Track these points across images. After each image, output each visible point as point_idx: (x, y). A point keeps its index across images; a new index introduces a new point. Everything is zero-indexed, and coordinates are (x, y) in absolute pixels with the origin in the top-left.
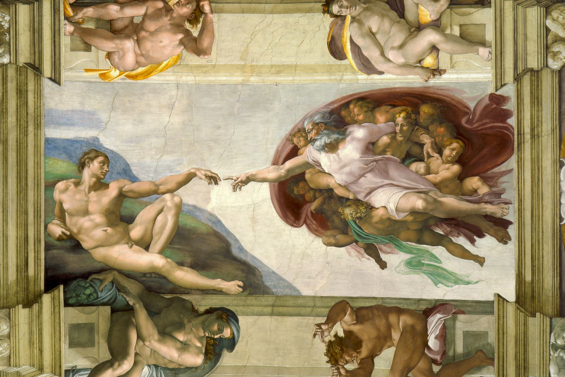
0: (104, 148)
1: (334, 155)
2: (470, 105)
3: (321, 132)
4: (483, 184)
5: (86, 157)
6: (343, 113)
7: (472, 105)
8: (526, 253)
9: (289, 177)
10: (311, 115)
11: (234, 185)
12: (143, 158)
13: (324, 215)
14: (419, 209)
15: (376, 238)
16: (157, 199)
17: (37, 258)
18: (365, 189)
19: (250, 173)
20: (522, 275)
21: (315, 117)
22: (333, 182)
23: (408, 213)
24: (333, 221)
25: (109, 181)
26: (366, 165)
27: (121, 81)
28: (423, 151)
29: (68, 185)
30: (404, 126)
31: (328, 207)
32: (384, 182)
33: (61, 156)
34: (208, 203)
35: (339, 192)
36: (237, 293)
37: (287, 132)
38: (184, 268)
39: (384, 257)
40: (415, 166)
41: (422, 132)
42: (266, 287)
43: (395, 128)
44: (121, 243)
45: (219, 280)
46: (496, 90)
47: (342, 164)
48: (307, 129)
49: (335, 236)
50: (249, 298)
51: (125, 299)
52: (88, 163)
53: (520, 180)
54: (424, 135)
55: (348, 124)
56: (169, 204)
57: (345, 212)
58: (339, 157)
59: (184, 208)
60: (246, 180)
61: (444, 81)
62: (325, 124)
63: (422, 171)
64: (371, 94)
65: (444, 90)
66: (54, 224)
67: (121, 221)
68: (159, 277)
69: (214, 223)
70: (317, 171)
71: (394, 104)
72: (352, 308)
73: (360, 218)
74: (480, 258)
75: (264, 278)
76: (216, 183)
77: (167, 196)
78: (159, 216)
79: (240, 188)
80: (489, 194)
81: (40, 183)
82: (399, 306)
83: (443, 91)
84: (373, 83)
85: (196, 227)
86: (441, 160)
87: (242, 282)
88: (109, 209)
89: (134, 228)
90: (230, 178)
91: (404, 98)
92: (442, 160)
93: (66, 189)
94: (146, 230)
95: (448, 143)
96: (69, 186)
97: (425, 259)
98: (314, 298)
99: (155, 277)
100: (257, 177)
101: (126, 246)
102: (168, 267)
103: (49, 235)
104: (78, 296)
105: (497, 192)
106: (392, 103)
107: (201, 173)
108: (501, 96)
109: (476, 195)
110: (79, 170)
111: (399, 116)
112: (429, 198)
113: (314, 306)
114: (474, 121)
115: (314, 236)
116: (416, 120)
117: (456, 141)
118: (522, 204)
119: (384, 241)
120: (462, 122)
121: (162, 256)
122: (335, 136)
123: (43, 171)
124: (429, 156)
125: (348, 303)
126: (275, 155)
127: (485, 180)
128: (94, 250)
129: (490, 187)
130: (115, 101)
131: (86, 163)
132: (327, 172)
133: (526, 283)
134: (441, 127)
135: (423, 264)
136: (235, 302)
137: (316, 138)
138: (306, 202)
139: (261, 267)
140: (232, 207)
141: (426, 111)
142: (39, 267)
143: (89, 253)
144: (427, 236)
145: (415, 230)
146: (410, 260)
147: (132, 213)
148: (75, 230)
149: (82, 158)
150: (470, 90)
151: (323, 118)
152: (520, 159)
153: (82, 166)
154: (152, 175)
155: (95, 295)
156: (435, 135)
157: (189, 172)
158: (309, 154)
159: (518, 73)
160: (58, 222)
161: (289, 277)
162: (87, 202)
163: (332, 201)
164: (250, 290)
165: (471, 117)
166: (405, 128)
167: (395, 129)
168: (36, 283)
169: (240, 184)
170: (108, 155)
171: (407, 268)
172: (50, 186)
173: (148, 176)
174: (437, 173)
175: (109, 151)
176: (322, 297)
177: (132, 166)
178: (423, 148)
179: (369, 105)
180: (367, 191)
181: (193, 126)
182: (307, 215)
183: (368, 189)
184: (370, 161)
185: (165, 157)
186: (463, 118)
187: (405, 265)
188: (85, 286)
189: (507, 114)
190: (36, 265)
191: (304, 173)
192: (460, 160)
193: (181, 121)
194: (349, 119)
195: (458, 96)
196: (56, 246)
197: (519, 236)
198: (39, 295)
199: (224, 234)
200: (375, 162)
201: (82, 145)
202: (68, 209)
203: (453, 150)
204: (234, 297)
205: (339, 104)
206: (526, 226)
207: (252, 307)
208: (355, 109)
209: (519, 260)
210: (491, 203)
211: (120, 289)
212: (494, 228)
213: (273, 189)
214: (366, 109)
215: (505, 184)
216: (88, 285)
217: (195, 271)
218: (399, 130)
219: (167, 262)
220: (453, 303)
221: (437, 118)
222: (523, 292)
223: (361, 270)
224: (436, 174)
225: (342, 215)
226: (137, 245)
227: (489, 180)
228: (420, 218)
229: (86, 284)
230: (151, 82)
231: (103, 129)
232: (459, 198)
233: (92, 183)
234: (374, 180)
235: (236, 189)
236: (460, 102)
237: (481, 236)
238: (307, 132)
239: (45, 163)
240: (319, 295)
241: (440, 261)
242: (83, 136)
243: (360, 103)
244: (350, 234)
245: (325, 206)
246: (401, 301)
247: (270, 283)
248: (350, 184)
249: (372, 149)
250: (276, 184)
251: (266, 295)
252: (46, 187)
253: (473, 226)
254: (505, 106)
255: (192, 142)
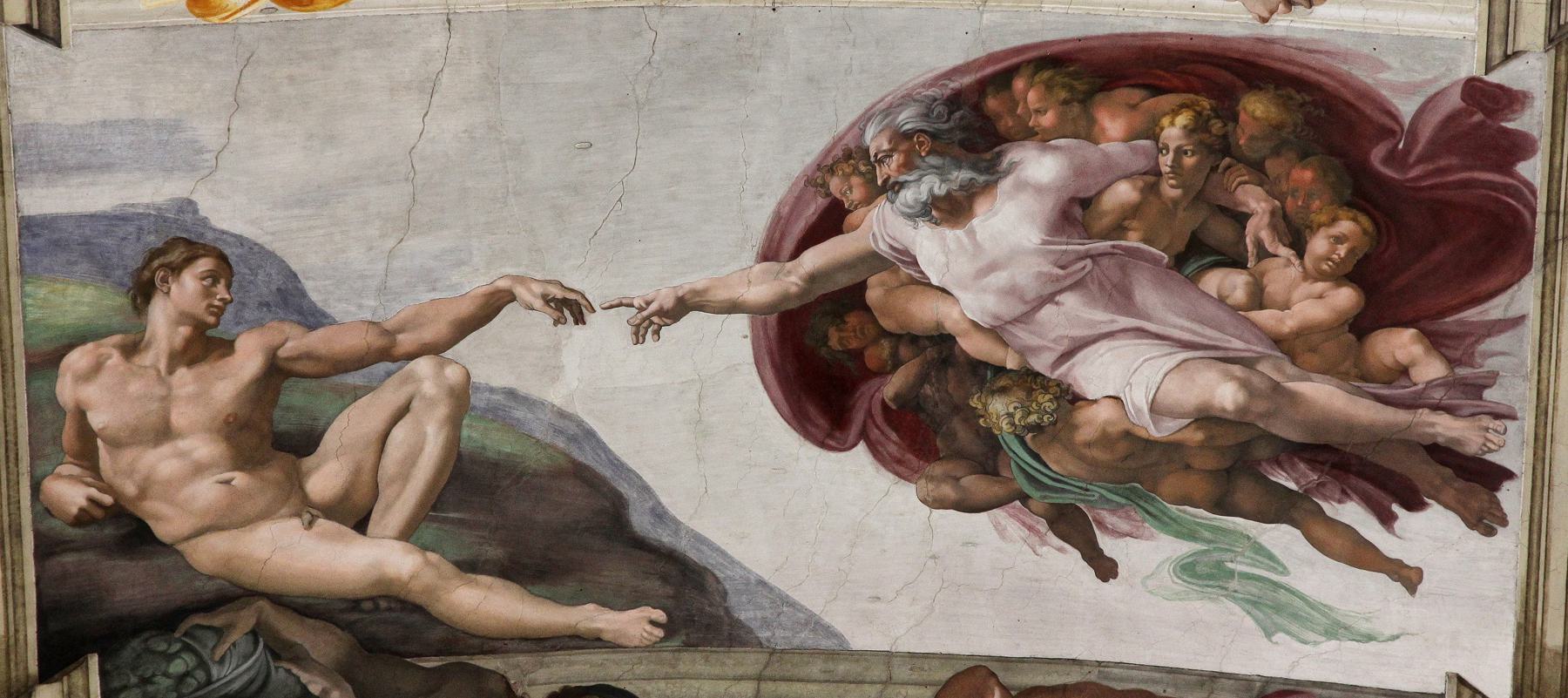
0: (215, 230)
1: (959, 232)
2: (1400, 107)
3: (918, 162)
4: (1427, 351)
5: (156, 263)
6: (992, 103)
7: (1407, 109)
8: (1552, 567)
9: (812, 298)
10: (888, 108)
11: (638, 321)
12: (344, 252)
13: (922, 416)
14: (1224, 410)
15: (1087, 490)
16: (389, 374)
17: (14, 585)
18: (1054, 341)
19: (687, 287)
20: (1535, 628)
21: (900, 113)
22: (955, 314)
23: (1190, 421)
24: (952, 436)
25: (234, 332)
26: (1063, 267)
27: (263, 18)
28: (1242, 237)
29: (102, 355)
30: (1186, 153)
31: (938, 390)
32: (1117, 322)
33: (75, 268)
34: (555, 379)
35: (975, 346)
36: (648, 643)
37: (809, 160)
38: (485, 579)
39: (1108, 545)
40: (1214, 281)
41: (1243, 178)
42: (737, 624)
43: (1157, 157)
44: (279, 515)
45: (590, 607)
46: (1488, 70)
47: (981, 263)
48: (872, 153)
49: (958, 479)
50: (686, 656)
51: (298, 678)
52: (164, 280)
53: (1546, 352)
54: (1249, 187)
55: (1007, 141)
56: (429, 388)
57: (991, 408)
58: (975, 239)
59: (477, 400)
60: (673, 309)
61: (1320, 27)
62: (934, 136)
63: (1239, 295)
64: (1082, 50)
65: (1320, 52)
66: (60, 476)
67: (276, 449)
68: (402, 610)
69: (573, 439)
70: (905, 280)
71: (1157, 82)
72: (1005, 689)
73: (1037, 428)
74: (1406, 570)
75: (733, 600)
76: (579, 319)
77: (423, 366)
78: (399, 423)
79: (657, 332)
80: (1448, 384)
81: (9, 361)
82: (1152, 689)
83: (1318, 56)
84: (1088, 13)
85: (516, 455)
86: (1300, 269)
87: (664, 611)
88: (236, 416)
89: (318, 467)
90: (624, 301)
91: (1189, 67)
92: (1304, 268)
93: (97, 368)
94: (357, 472)
95: (1323, 218)
96: (104, 357)
97: (1239, 559)
98: (889, 656)
99: (390, 609)
100: (711, 299)
101: (296, 522)
102: (428, 577)
103: (47, 511)
104: (146, 681)
105: (1471, 382)
106: (1148, 81)
107: (530, 290)
108: (1500, 87)
109: (1403, 382)
110: (136, 307)
111: (1172, 124)
112: (1256, 380)
113: (888, 681)
114: (1412, 159)
115: (891, 476)
116: (1225, 136)
117: (1351, 215)
118: (1546, 423)
119: (1112, 501)
120: (1372, 157)
121: (408, 544)
122: (963, 175)
123: (17, 320)
124: (1263, 254)
125: (993, 675)
126: (769, 230)
127: (1436, 341)
128: (194, 541)
129: (1452, 362)
130: (243, 81)
131: (158, 282)
132: (935, 282)
133: (1547, 655)
134: (1304, 168)
135: (1231, 574)
136: (641, 669)
137: (902, 178)
138: (868, 374)
139: (722, 565)
140: (630, 389)
141: (1258, 113)
142: (20, 610)
143: (178, 552)
144: (1245, 492)
145: (1210, 472)
146: (1190, 560)
147: (310, 422)
148: (130, 489)
149: (143, 268)
150: (1401, 62)
151: (926, 116)
152: (1548, 287)
153: (143, 292)
154: (372, 303)
155: (200, 675)
156: (1285, 189)
157: (490, 289)
158: (880, 230)
159: (1562, 22)
160: (76, 470)
161: (811, 598)
162: (166, 400)
163: (951, 372)
164: (687, 635)
165: (1401, 146)
166: (1189, 161)
167: (1158, 164)
168: (13, 657)
169: (655, 319)
170: (227, 251)
171: (1180, 582)
172: (46, 362)
173: (360, 306)
174: (1286, 306)
175: (232, 239)
176: (912, 655)
177: (307, 279)
178: (1245, 228)
179: (1075, 83)
180: (1061, 349)
181: (502, 143)
182: (869, 414)
183: (1066, 342)
184: (1072, 257)
185: (409, 243)
186: (1378, 144)
187: (1174, 572)
188: (169, 651)
189: (1520, 146)
190: (11, 604)
191: (862, 287)
192: (1356, 273)
193: (464, 128)
194: (1010, 124)
195: (1362, 75)
196: (72, 541)
197: (1531, 516)
198: (23, 690)
199: (607, 473)
200: (1088, 262)
201: (140, 229)
202: (103, 429)
203: (1339, 240)
204: (639, 655)
205: (979, 75)
206: (1556, 490)
207: (693, 681)
208: (1030, 94)
209: (1528, 585)
210: (1450, 410)
211: (280, 650)
212: (1456, 485)
213: (761, 333)
214: (1063, 95)
215: (1501, 359)
216: (176, 647)
217: (514, 587)
218: (1171, 167)
219: (427, 563)
220: (1318, 691)
221: (1292, 137)
222: (1536, 676)
223: (1037, 580)
224: (1282, 311)
225: (982, 416)
226: (330, 519)
227: (1447, 342)
228: (1229, 439)
229: (170, 645)
230: (360, 12)
231: (207, 172)
232: (1349, 387)
233: (178, 341)
234: (1085, 315)
235: (644, 337)
236: (1368, 95)
237: (1414, 503)
238: (872, 159)
239: (24, 295)
240: (906, 646)
241: (1285, 568)
242: (146, 200)
243: (1046, 75)
244: (1005, 473)
245: (928, 389)
246: (1157, 675)
247: (751, 614)
248: (1010, 322)
249: (1080, 219)
250: (772, 319)
251: (736, 649)
252: (31, 368)
253: (1390, 473)
254: (1514, 120)
255: (500, 196)
